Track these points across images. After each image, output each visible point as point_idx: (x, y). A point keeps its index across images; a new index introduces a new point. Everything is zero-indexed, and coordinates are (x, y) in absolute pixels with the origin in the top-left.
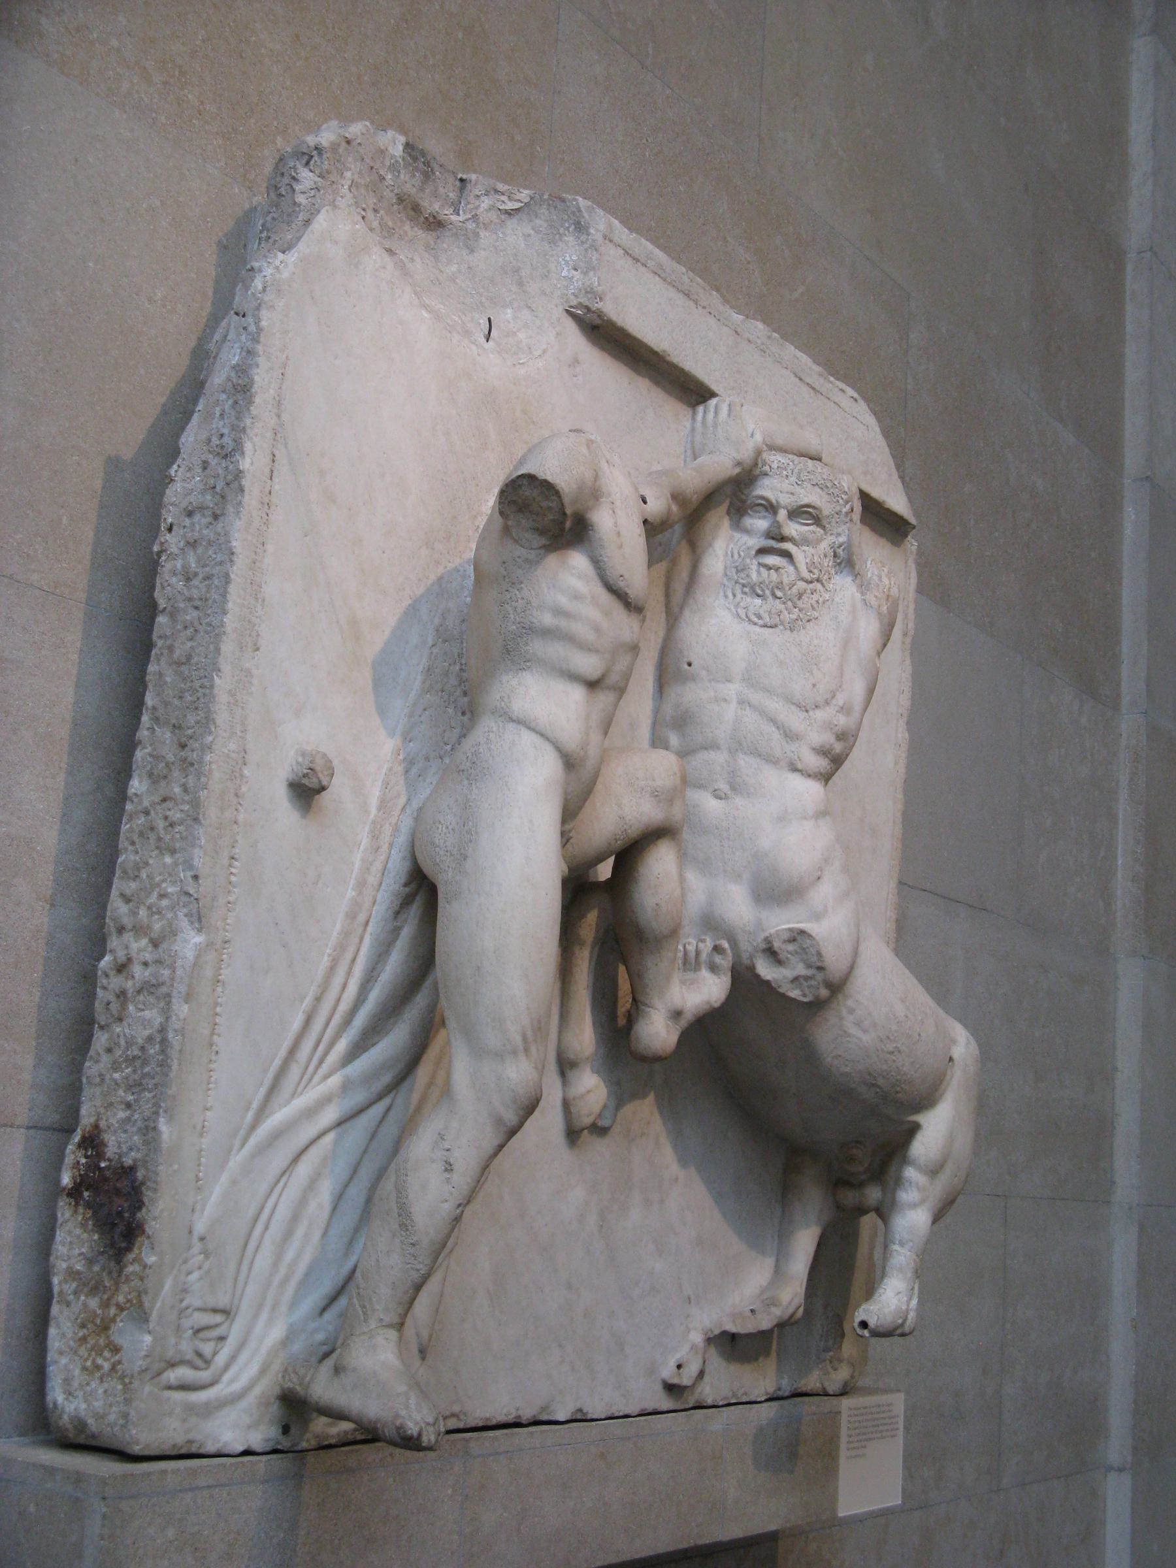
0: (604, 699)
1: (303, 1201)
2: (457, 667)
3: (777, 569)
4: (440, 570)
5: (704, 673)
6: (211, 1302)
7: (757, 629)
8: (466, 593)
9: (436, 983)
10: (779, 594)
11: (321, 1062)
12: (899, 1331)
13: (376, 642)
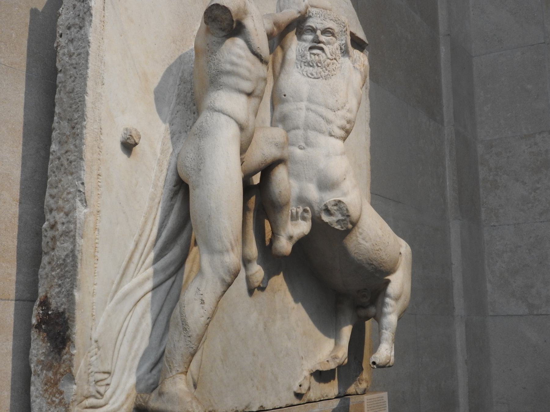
0: (254, 101)
1: (139, 324)
2: (190, 94)
3: (318, 55)
4: (180, 54)
5: (291, 99)
6: (102, 369)
7: (312, 80)
8: (192, 62)
9: (191, 225)
10: (319, 65)
11: (144, 262)
12: (388, 365)
13: (155, 82)
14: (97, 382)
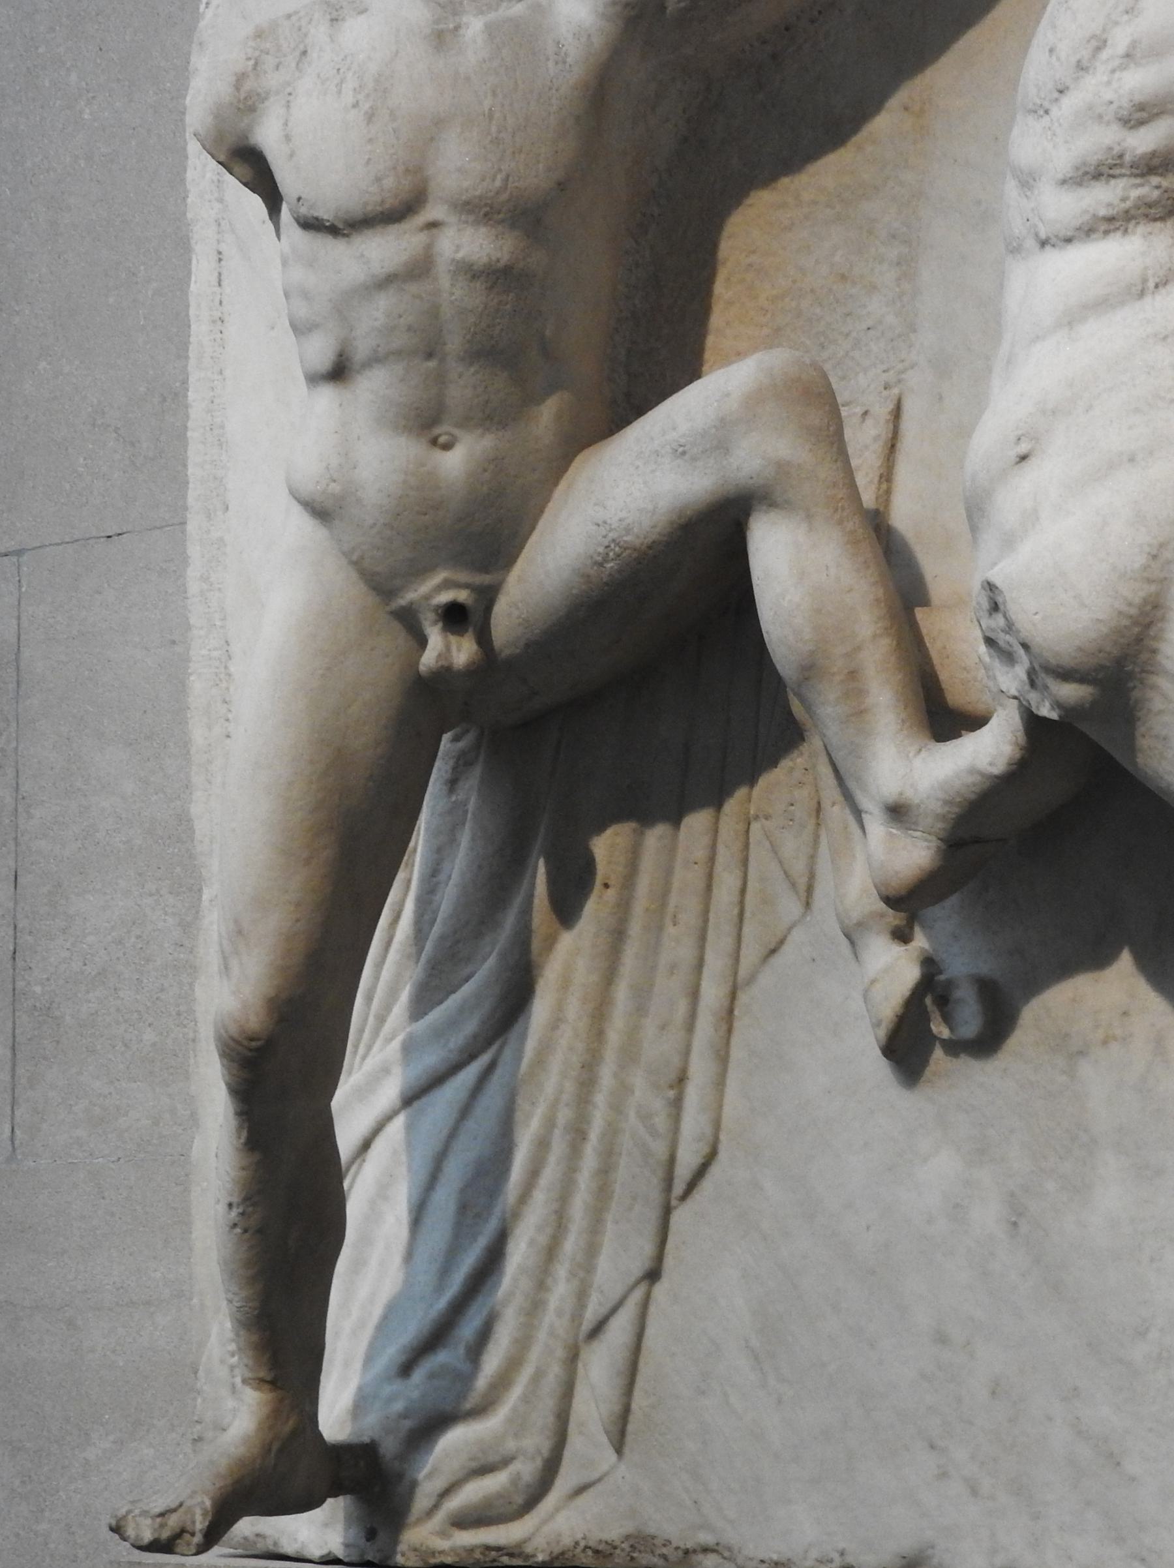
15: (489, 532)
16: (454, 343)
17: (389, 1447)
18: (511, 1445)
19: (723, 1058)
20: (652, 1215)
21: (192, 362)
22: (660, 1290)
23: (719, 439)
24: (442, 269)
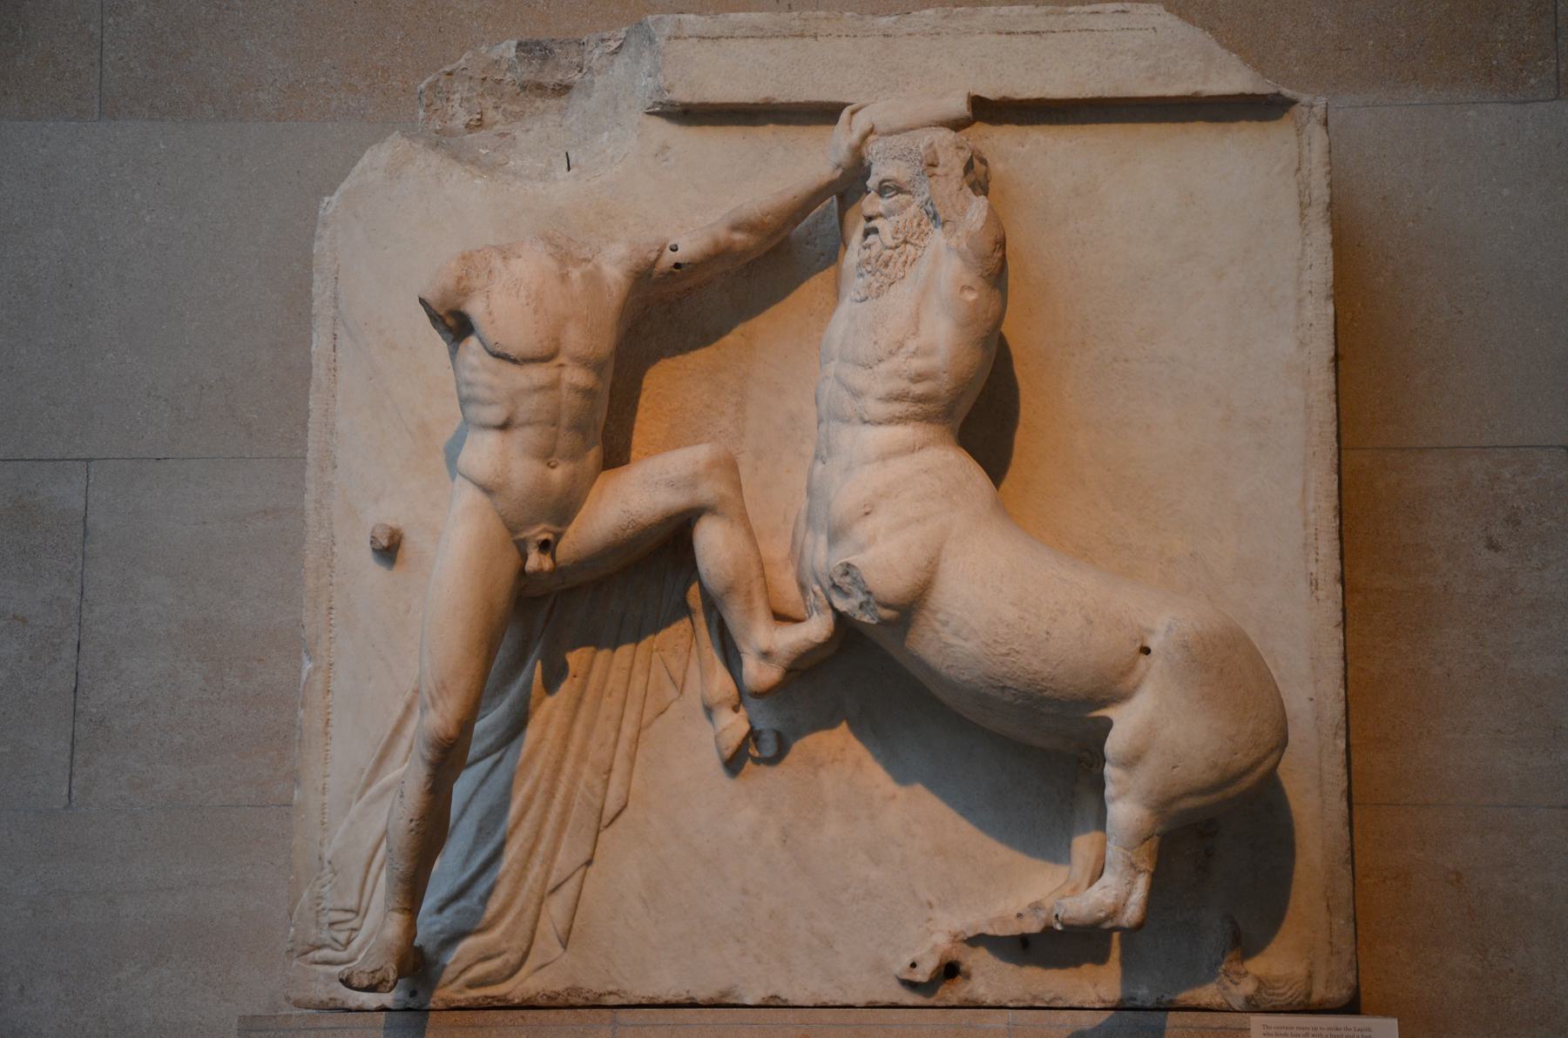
6: (340, 905)
14: (332, 924)
15: (564, 509)
16: (565, 421)
17: (430, 948)
18: (504, 945)
19: (632, 760)
20: (593, 834)
21: (312, 389)
22: (592, 870)
23: (693, 481)
24: (564, 385)
